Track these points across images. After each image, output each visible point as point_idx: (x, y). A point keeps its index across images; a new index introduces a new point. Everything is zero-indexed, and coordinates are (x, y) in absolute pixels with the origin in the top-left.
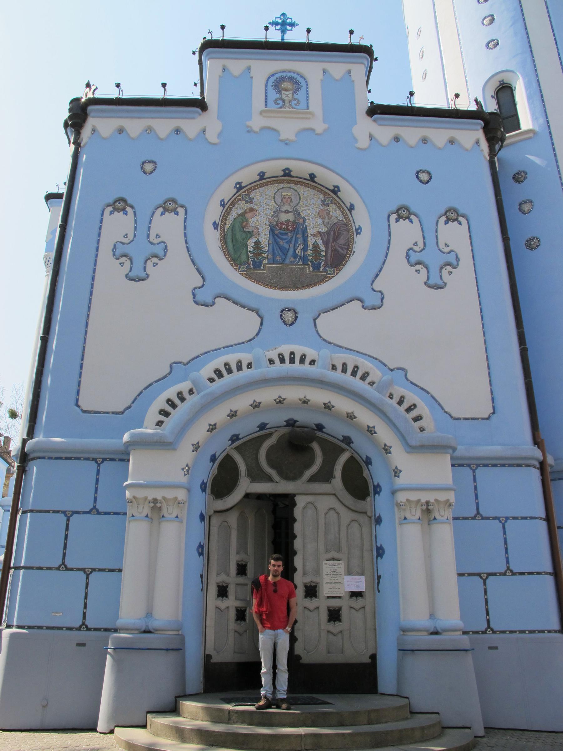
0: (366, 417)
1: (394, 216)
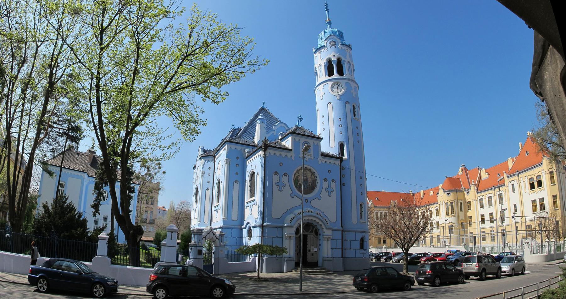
0: (321, 223)
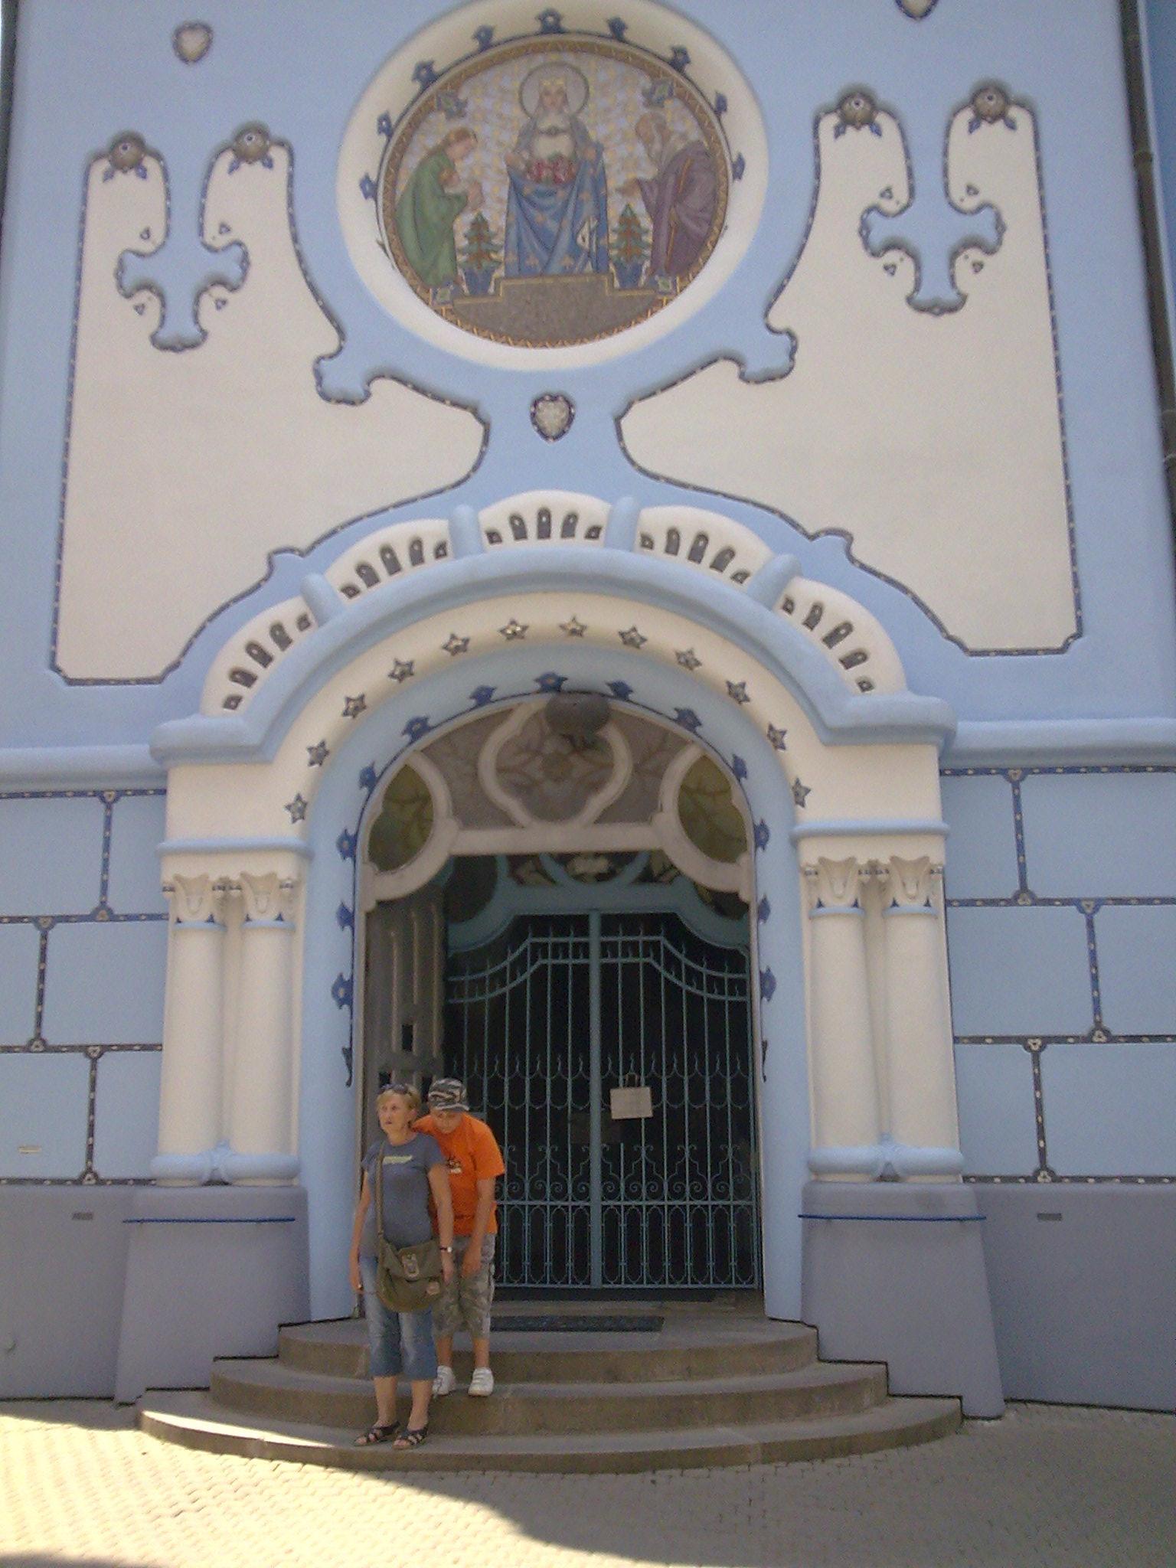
0: (722, 662)
1: (830, 122)
